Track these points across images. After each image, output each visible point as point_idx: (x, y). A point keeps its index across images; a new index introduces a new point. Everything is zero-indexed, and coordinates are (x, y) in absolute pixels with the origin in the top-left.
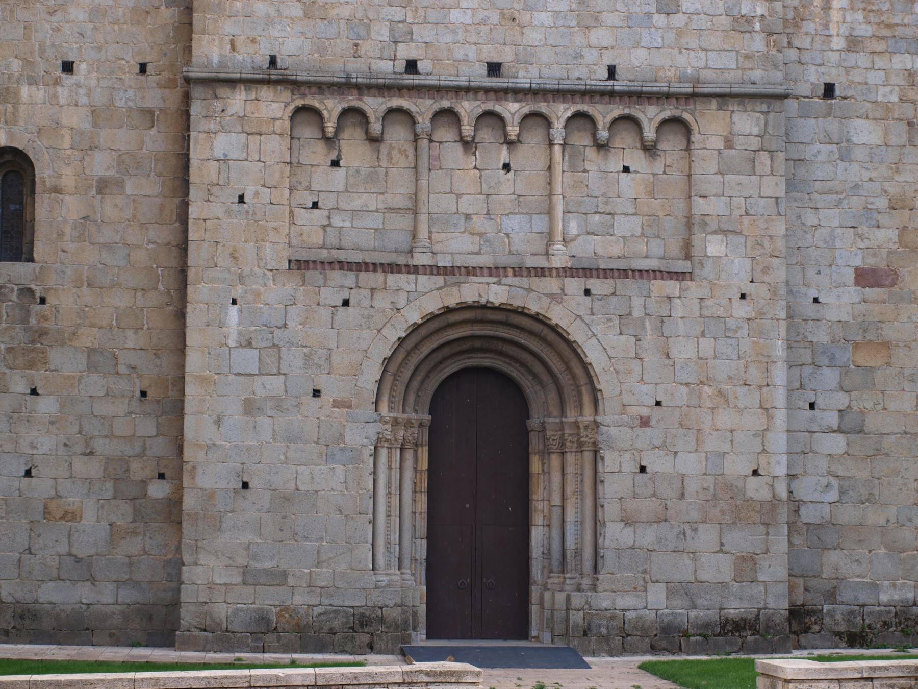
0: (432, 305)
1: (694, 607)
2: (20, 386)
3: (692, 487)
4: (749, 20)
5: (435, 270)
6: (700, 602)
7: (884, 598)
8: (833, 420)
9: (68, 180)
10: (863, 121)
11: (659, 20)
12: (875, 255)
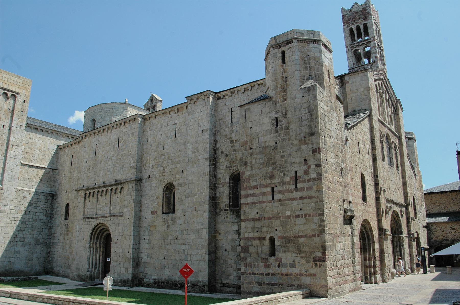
0: (95, 224)
1: (120, 277)
2: (66, 239)
3: (121, 255)
4: (132, 167)
5: (97, 218)
6: (121, 277)
7: (153, 278)
8: (146, 241)
9: (72, 208)
10: (153, 182)
11: (121, 169)
12: (154, 208)
